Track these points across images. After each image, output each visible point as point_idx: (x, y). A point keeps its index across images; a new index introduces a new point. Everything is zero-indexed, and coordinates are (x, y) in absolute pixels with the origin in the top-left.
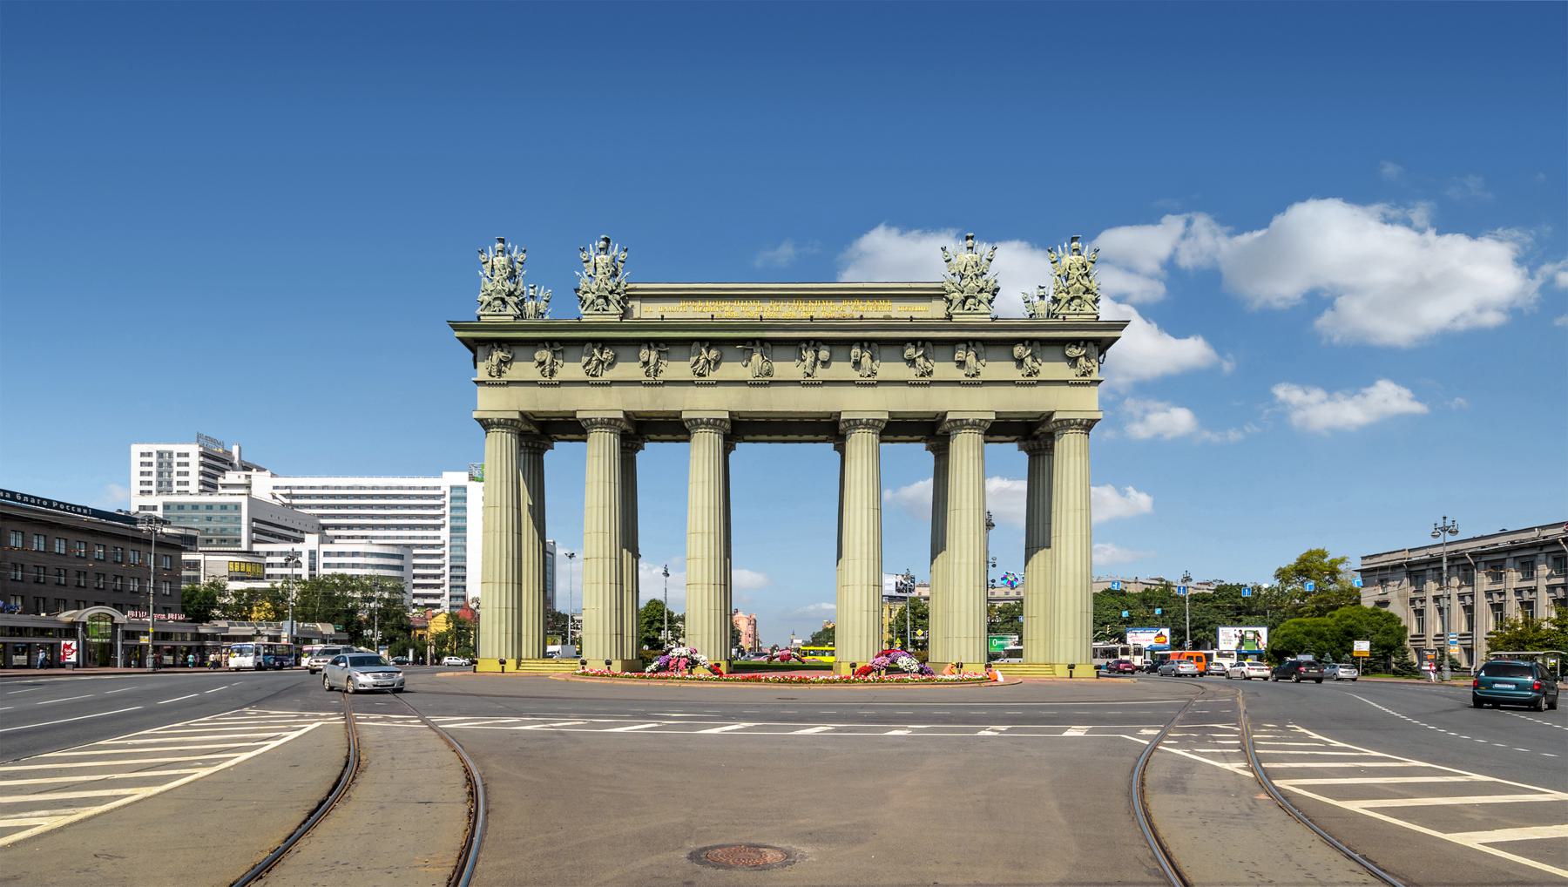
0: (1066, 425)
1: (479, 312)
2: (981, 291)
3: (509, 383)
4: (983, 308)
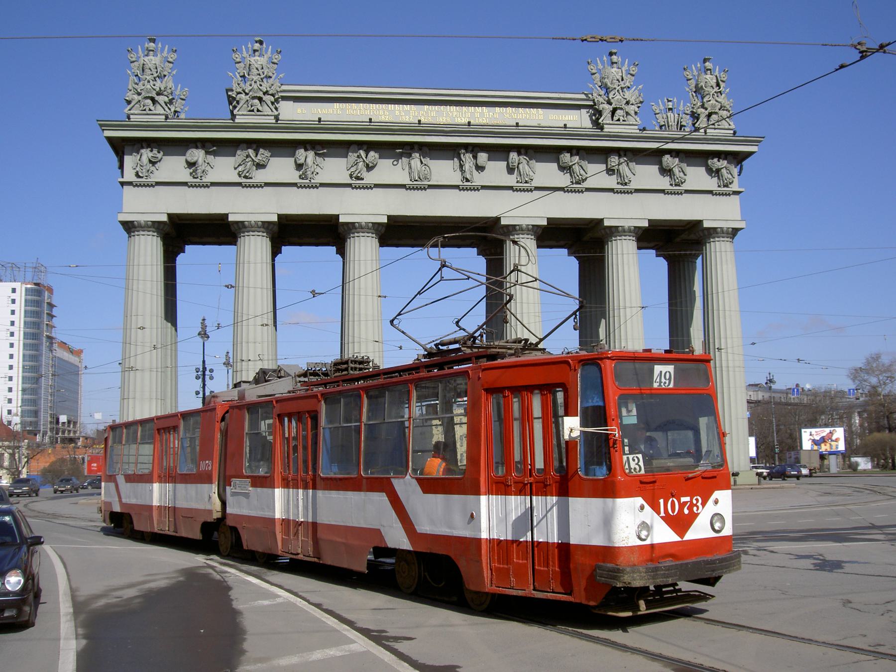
1: (126, 111)
2: (628, 103)
3: (158, 184)
4: (631, 120)
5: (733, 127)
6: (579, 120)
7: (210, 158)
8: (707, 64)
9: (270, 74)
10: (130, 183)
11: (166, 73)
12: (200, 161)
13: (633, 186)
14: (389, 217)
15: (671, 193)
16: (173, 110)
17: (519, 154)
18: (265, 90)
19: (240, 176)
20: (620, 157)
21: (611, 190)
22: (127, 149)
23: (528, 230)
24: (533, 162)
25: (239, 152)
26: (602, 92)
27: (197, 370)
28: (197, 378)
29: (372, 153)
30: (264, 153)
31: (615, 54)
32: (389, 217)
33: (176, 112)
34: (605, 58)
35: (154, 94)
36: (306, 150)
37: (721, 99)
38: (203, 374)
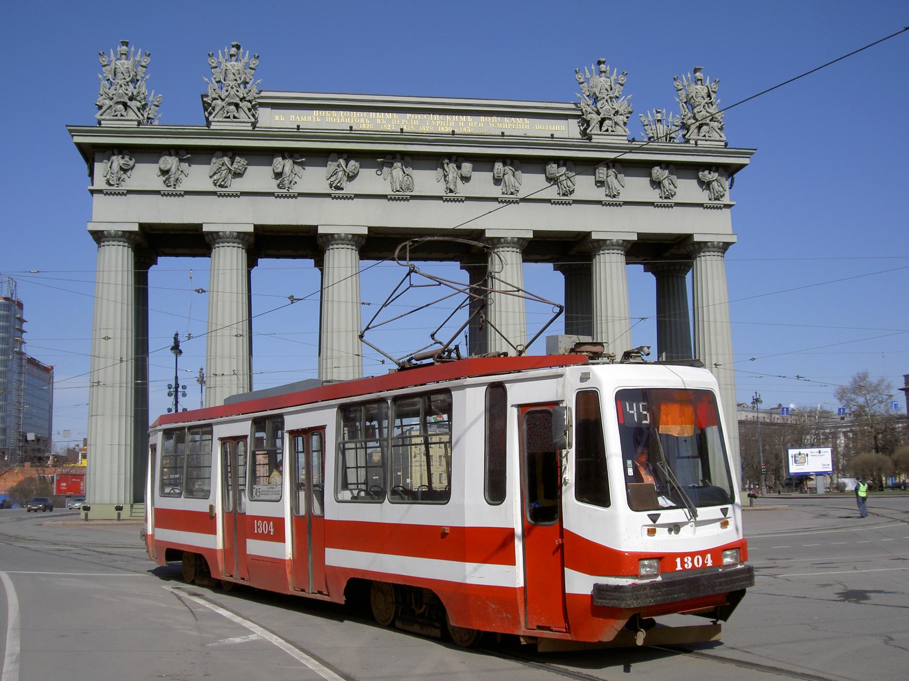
0: (702, 246)
1: (98, 116)
3: (130, 192)
4: (619, 130)
5: (724, 138)
6: (569, 130)
7: (184, 166)
8: (698, 74)
9: (248, 80)
10: (100, 191)
11: (138, 77)
12: (173, 170)
13: (621, 198)
14: (370, 228)
15: (661, 206)
16: (146, 116)
17: (505, 164)
18: (242, 96)
19: (215, 185)
20: (608, 168)
21: (599, 202)
22: (97, 157)
23: (514, 243)
24: (519, 173)
25: (214, 160)
26: (590, 102)
27: (170, 387)
28: (170, 394)
29: (352, 163)
30: (240, 162)
31: (604, 63)
32: (370, 228)
33: (148, 118)
34: (593, 67)
35: (126, 99)
36: (284, 158)
37: (713, 110)
38: (176, 390)
